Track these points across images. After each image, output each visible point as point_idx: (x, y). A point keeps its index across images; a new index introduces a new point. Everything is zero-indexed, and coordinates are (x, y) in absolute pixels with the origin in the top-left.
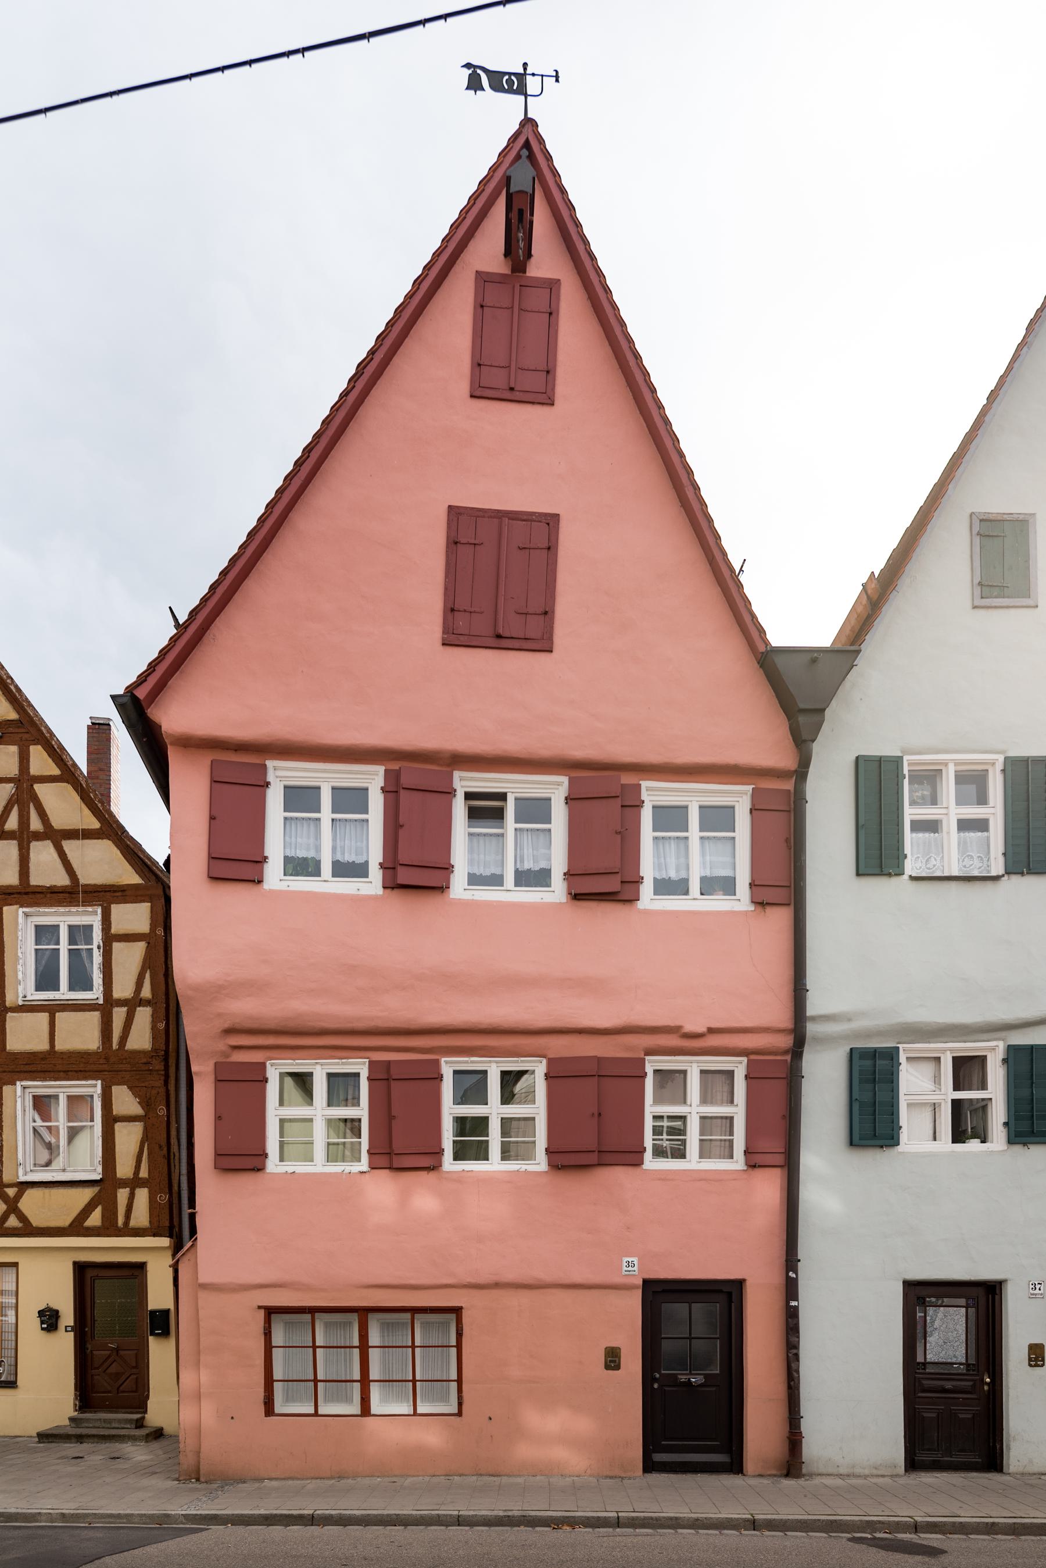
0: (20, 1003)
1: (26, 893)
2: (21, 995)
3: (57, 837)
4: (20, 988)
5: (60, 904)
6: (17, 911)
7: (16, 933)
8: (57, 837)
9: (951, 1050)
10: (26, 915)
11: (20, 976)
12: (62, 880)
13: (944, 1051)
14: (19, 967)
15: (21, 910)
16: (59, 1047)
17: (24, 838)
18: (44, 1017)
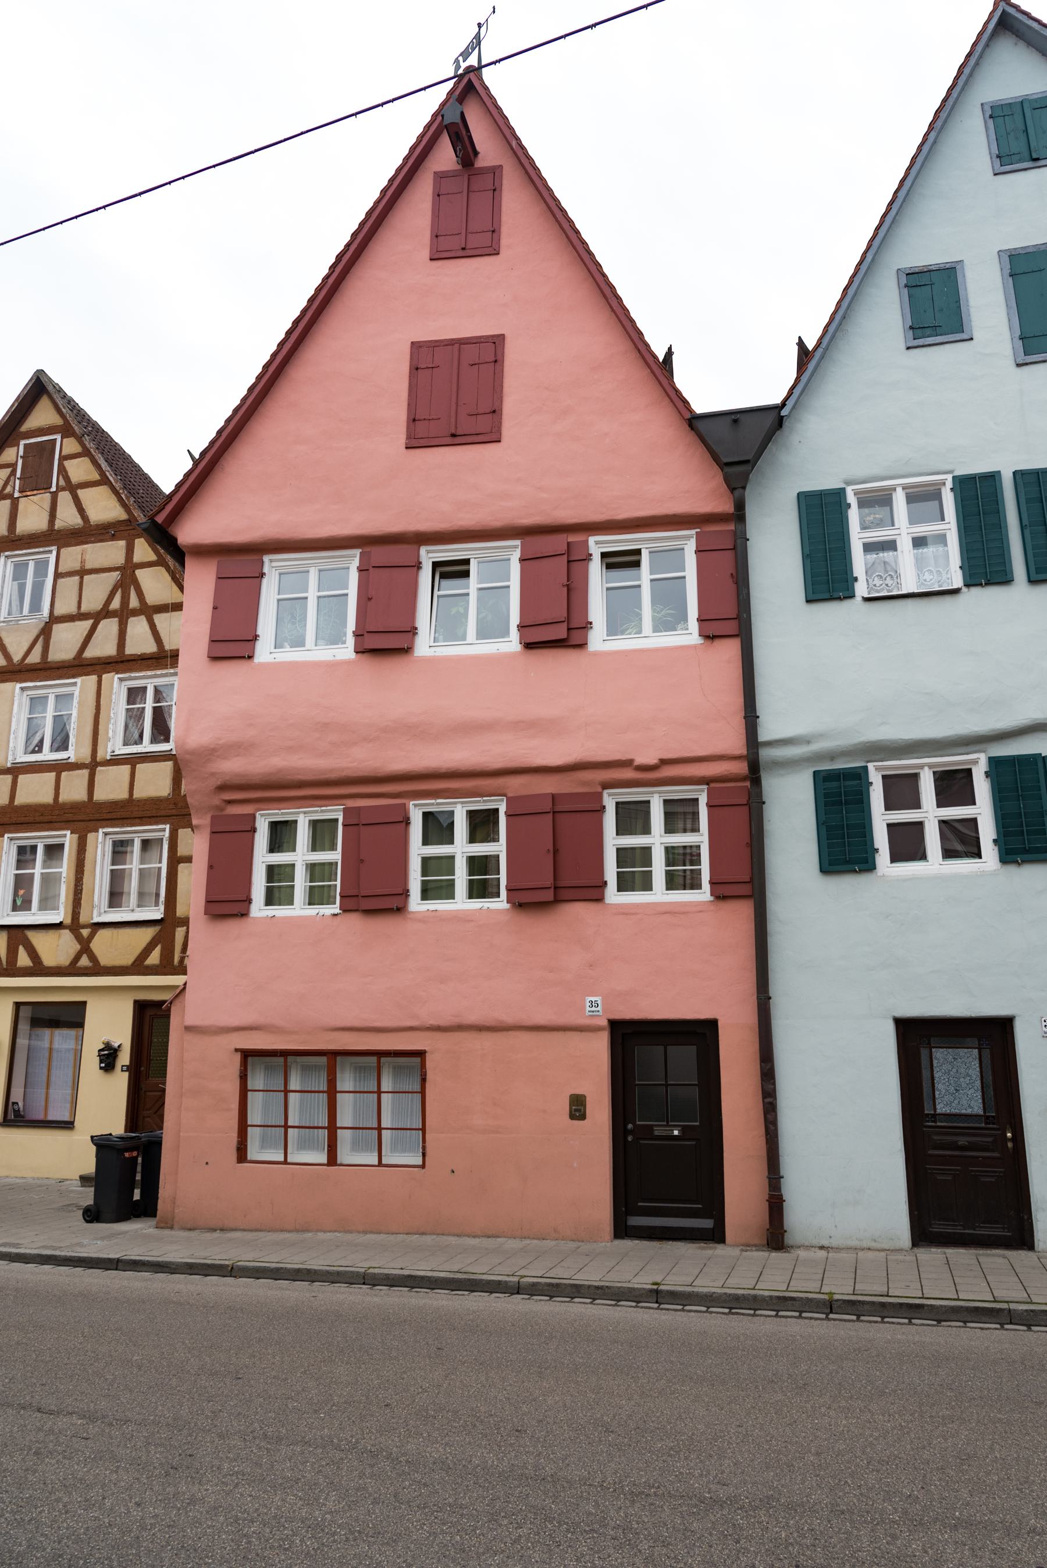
0: (108, 758)
1: (122, 662)
2: (109, 750)
3: (149, 611)
4: (110, 745)
5: (149, 668)
6: (113, 678)
7: (111, 696)
8: (149, 611)
9: (930, 766)
10: (121, 680)
11: (110, 734)
12: (151, 648)
13: (922, 767)
14: (111, 726)
15: (117, 676)
16: (137, 795)
17: (124, 615)
18: (126, 769)
